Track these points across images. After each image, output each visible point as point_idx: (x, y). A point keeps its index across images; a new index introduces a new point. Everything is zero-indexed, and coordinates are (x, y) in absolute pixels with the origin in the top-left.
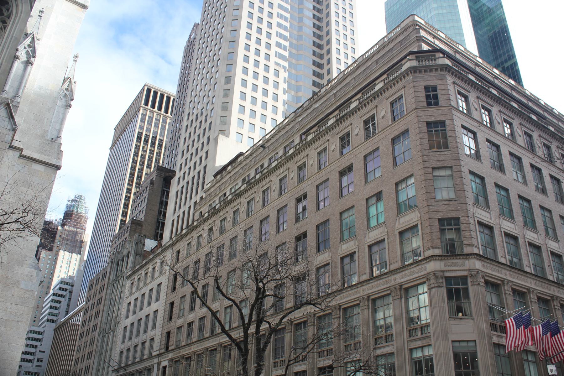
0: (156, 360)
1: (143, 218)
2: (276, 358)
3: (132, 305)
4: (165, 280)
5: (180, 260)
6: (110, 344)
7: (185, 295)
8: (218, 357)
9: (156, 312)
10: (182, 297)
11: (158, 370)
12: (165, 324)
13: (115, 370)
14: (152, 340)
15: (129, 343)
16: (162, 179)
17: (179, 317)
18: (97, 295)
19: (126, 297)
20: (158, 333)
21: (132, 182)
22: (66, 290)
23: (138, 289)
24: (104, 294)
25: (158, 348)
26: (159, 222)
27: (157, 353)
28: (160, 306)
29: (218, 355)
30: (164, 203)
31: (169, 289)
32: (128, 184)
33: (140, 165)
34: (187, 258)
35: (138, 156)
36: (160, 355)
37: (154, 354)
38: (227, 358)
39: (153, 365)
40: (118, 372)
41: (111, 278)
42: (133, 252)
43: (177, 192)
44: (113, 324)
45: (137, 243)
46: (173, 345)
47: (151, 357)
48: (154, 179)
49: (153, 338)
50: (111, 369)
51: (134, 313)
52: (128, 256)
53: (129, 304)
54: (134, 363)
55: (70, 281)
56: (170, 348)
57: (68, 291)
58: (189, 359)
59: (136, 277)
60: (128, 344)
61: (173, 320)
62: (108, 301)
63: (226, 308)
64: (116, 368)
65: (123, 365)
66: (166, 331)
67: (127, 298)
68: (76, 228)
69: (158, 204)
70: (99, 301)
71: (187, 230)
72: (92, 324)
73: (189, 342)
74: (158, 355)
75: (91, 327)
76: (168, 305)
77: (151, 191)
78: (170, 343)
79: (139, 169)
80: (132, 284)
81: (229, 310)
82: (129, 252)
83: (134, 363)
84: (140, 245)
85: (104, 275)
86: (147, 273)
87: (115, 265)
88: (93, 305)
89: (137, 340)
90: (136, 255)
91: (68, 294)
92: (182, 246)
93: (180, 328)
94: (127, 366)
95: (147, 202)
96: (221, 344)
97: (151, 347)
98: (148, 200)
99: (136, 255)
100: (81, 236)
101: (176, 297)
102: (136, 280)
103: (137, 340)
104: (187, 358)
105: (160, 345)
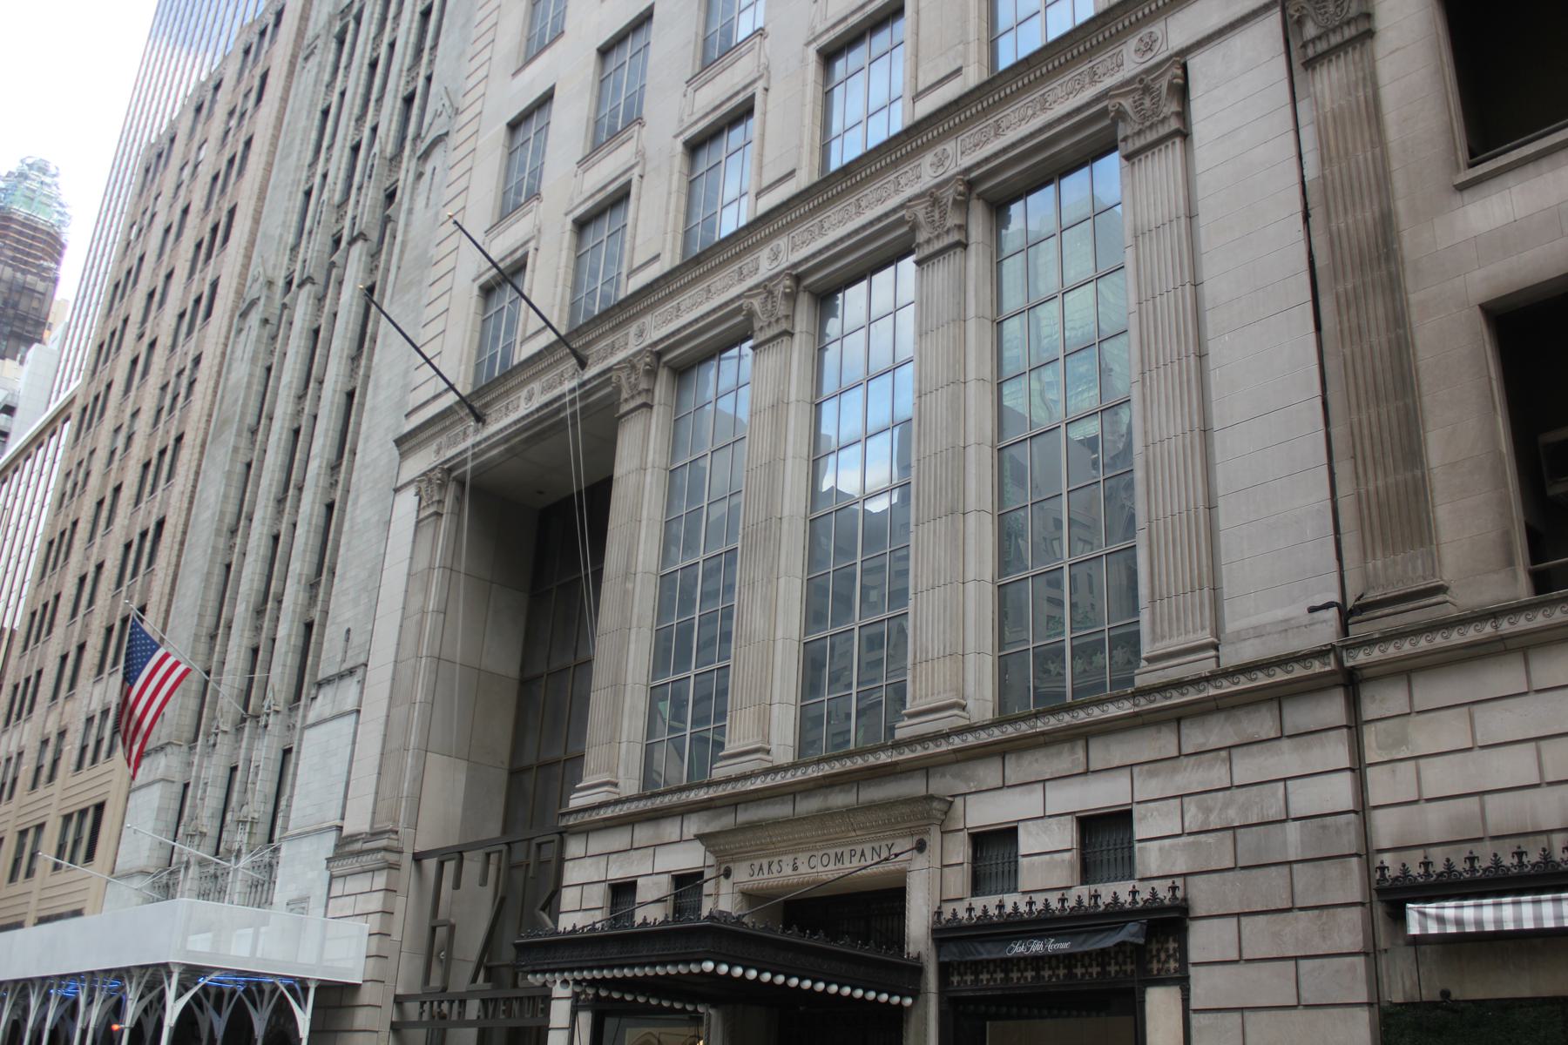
40: (480, 419)
68: (24, 272)
100: (41, 302)
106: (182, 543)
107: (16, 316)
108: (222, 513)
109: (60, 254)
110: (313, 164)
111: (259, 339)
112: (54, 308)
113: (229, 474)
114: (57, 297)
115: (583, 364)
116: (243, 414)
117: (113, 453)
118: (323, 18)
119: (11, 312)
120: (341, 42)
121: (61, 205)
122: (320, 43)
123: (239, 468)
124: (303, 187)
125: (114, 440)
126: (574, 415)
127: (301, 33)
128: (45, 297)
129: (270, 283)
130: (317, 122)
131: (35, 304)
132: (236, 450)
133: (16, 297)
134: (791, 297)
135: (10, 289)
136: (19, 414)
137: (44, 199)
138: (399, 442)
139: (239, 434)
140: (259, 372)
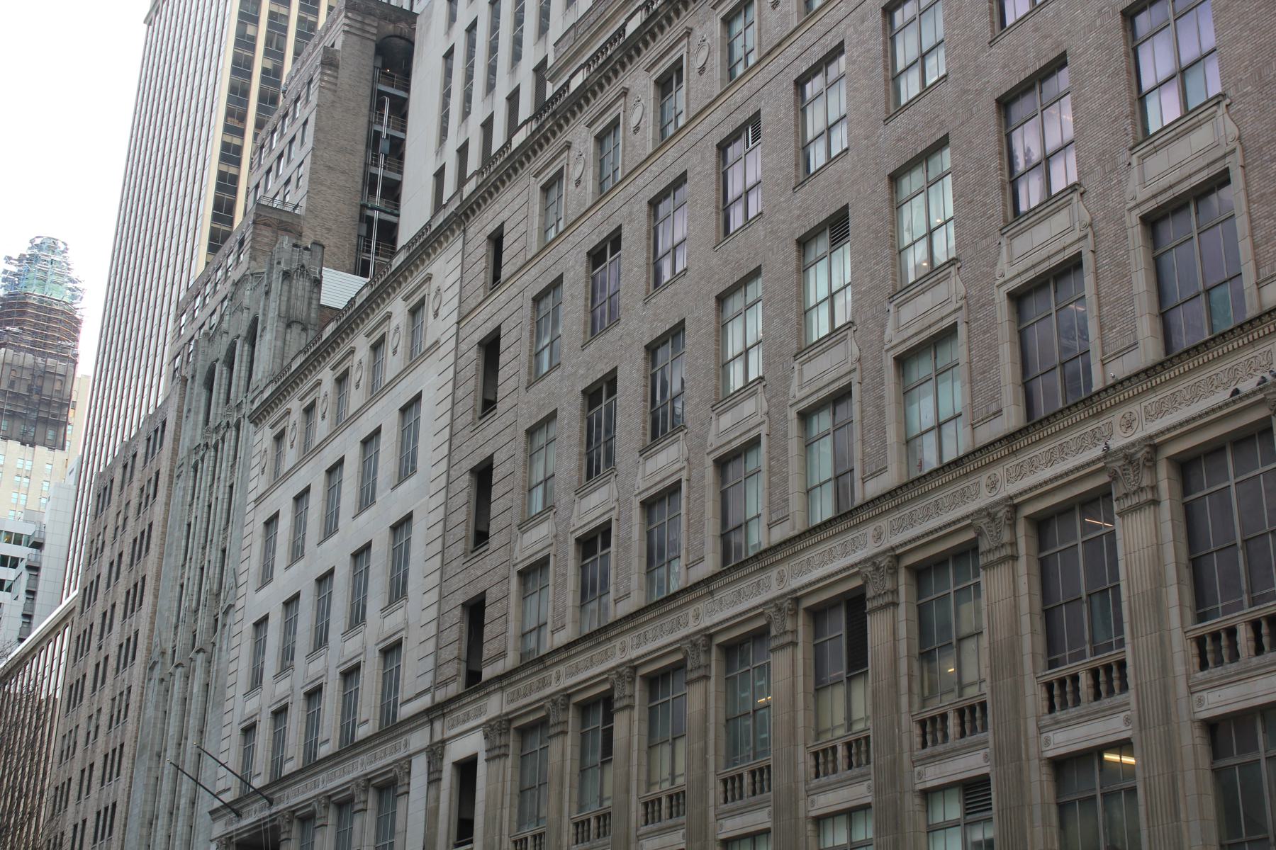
0: (419, 739)
1: (303, 204)
2: (1201, 618)
3: (285, 524)
4: (432, 381)
5: (506, 272)
6: (195, 706)
7: (553, 416)
8: (786, 669)
9: (402, 525)
10: (531, 432)
11: (434, 780)
12: (450, 570)
13: (226, 806)
14: (391, 650)
15: (283, 687)
16: (371, 48)
17: (526, 523)
18: (131, 522)
19: (253, 497)
20: (422, 619)
21: (242, 118)
22: (15, 563)
23: (309, 452)
24: (157, 512)
25: (427, 681)
26: (370, 220)
27: (425, 702)
28: (427, 495)
29: (780, 663)
30: (385, 145)
31: (460, 408)
32: (228, 129)
33: (267, 53)
34: (545, 247)
35: (256, 21)
36: (436, 712)
37: (405, 711)
38: (838, 666)
39: (405, 764)
40: (239, 815)
41: (185, 443)
42: (272, 313)
43: (449, 55)
44: (203, 621)
45: (287, 275)
46: (502, 655)
47: (391, 728)
48: (338, 46)
49: (398, 644)
50: (207, 803)
51: (297, 553)
52: (252, 338)
53: (271, 522)
54: (312, 765)
55: (27, 530)
56: (487, 673)
57: (22, 566)
58: (598, 706)
59: (295, 405)
60: (275, 690)
61: (494, 542)
62: (178, 534)
63: (805, 416)
64: (227, 797)
65: (257, 783)
66: (460, 598)
67: (258, 501)
68: (43, 355)
69: (362, 148)
70: (142, 543)
71: (534, 125)
72: (115, 638)
73: (591, 626)
74: (427, 711)
75: (113, 651)
76: (464, 483)
77: (330, 96)
78: (488, 650)
79: (265, 71)
80: (279, 438)
81: (823, 422)
82: (255, 320)
83: (312, 765)
84: (301, 285)
85: (155, 435)
86: (346, 374)
87: (198, 388)
88: (115, 566)
89: (316, 667)
90: (289, 326)
91: (26, 575)
92: (516, 207)
93: (533, 572)
94: (280, 781)
95: (317, 140)
96: (797, 600)
97: (390, 682)
98: (318, 129)
99: (289, 326)
100: (63, 383)
101: (500, 438)
102: (297, 416)
103: (316, 667)
104: (585, 708)
105: (437, 667)
106: (125, 826)
107: (41, 402)
108: (144, 812)
109: (77, 331)
110: (184, 565)
111: (158, 694)
112: (75, 387)
113: (146, 785)
114: (78, 375)
115: (271, 803)
116: (153, 745)
117: (89, 734)
118: (185, 453)
119: (35, 398)
120: (196, 471)
121: (72, 281)
122: (184, 469)
123: (152, 781)
124: (179, 582)
125: (89, 725)
126: (266, 830)
127: (175, 452)
128: (66, 378)
129: (163, 653)
130: (185, 533)
131: (57, 386)
132: (150, 769)
133: (39, 382)
134: (326, 807)
135: (33, 375)
136: (46, 547)
137: (54, 278)
138: (211, 813)
139: (151, 759)
140: (160, 715)
